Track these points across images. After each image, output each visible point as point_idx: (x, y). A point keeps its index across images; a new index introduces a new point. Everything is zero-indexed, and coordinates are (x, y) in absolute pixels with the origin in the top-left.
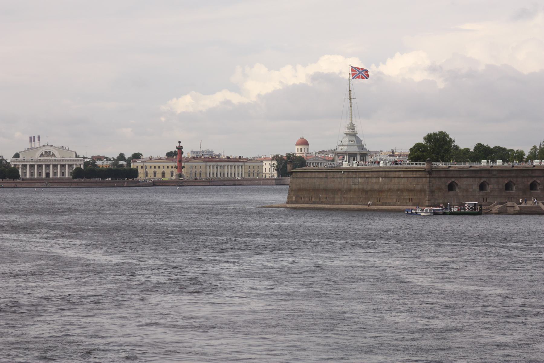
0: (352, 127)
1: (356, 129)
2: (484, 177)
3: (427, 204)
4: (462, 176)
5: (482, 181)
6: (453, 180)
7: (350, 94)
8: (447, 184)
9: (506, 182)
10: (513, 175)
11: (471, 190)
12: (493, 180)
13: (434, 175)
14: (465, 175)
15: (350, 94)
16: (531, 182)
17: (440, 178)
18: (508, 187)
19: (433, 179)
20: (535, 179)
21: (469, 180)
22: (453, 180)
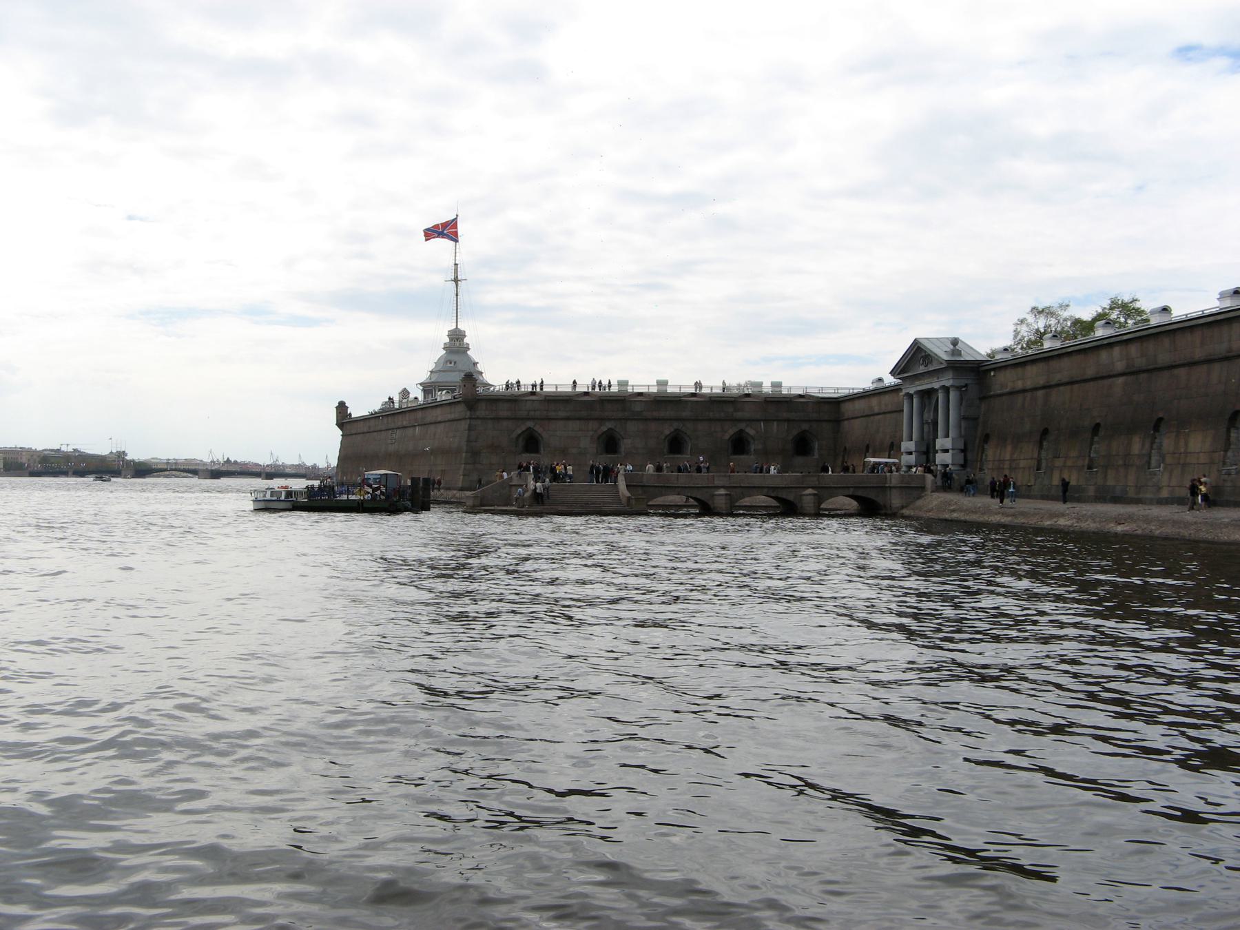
0: (457, 337)
1: (466, 340)
2: (609, 420)
3: (460, 485)
4: (552, 414)
5: (604, 429)
6: (530, 424)
7: (456, 271)
8: (514, 435)
9: (667, 432)
10: (686, 414)
11: (574, 451)
12: (632, 427)
13: (482, 411)
14: (562, 414)
15: (456, 271)
16: (731, 432)
17: (497, 419)
18: (676, 444)
19: (479, 422)
20: (742, 426)
21: (571, 424)
22: (530, 424)
